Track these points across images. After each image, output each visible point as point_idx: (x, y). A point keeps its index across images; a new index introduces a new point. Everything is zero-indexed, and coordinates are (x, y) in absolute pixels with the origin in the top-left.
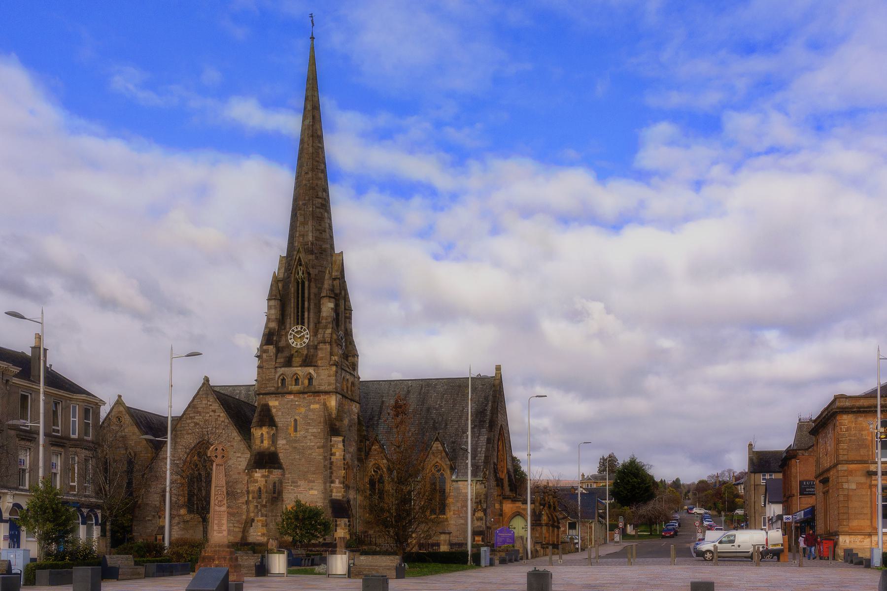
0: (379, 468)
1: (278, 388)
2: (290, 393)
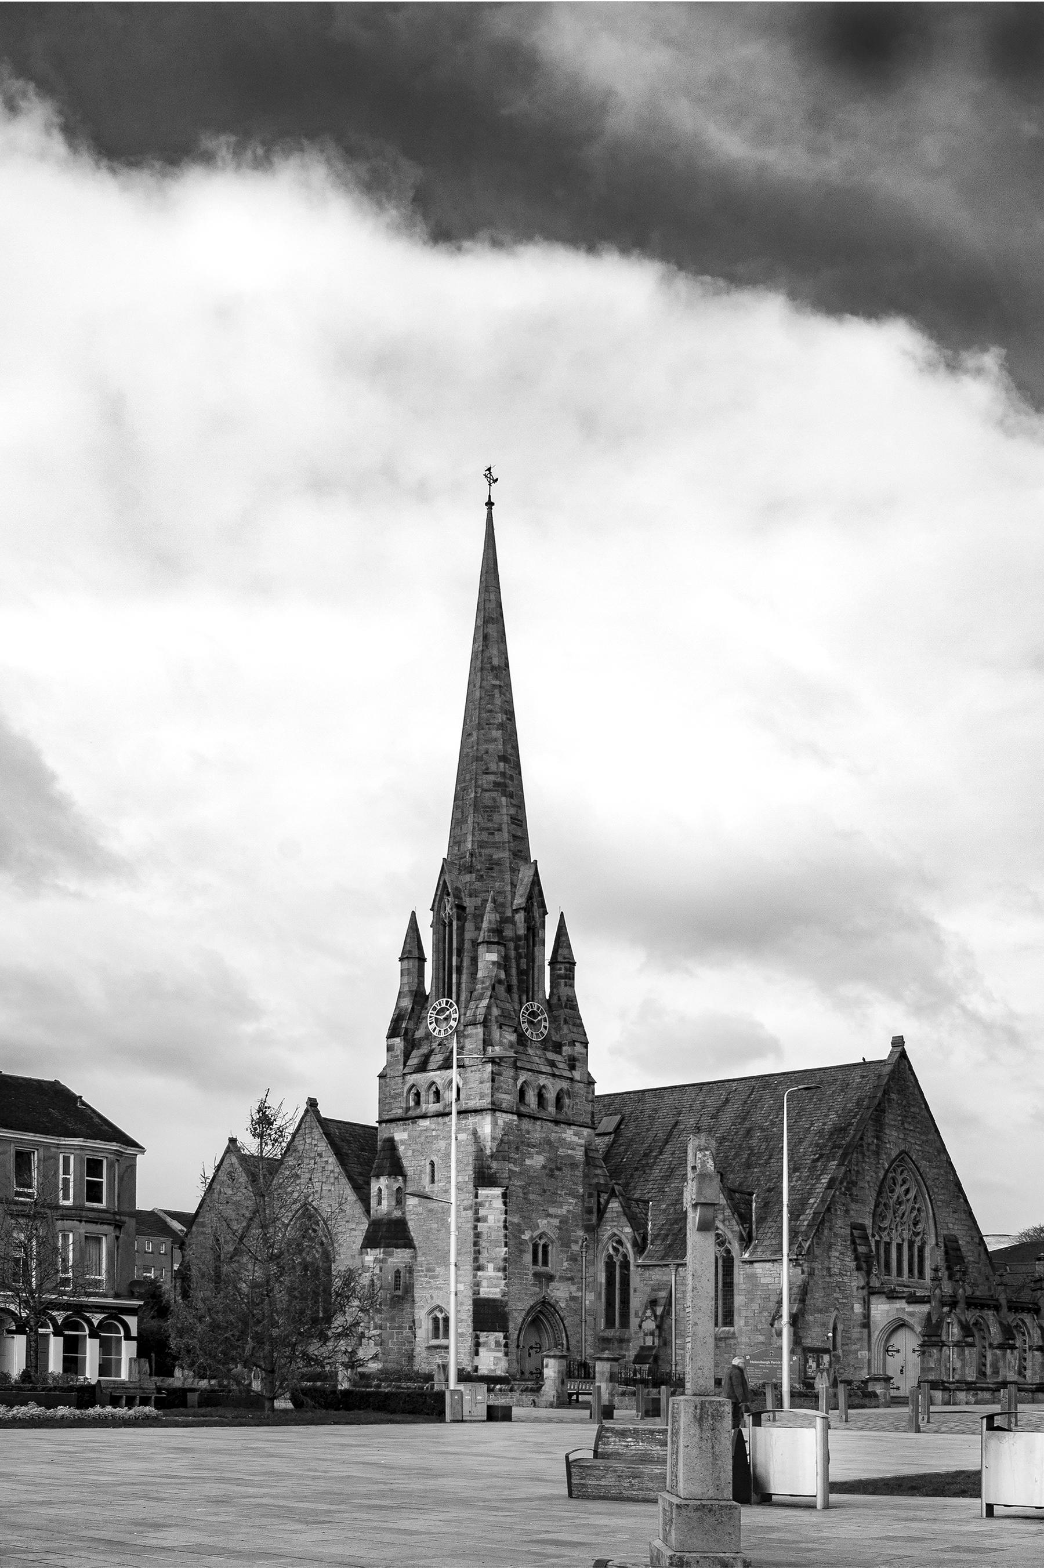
1: (408, 1109)
2: (424, 1117)
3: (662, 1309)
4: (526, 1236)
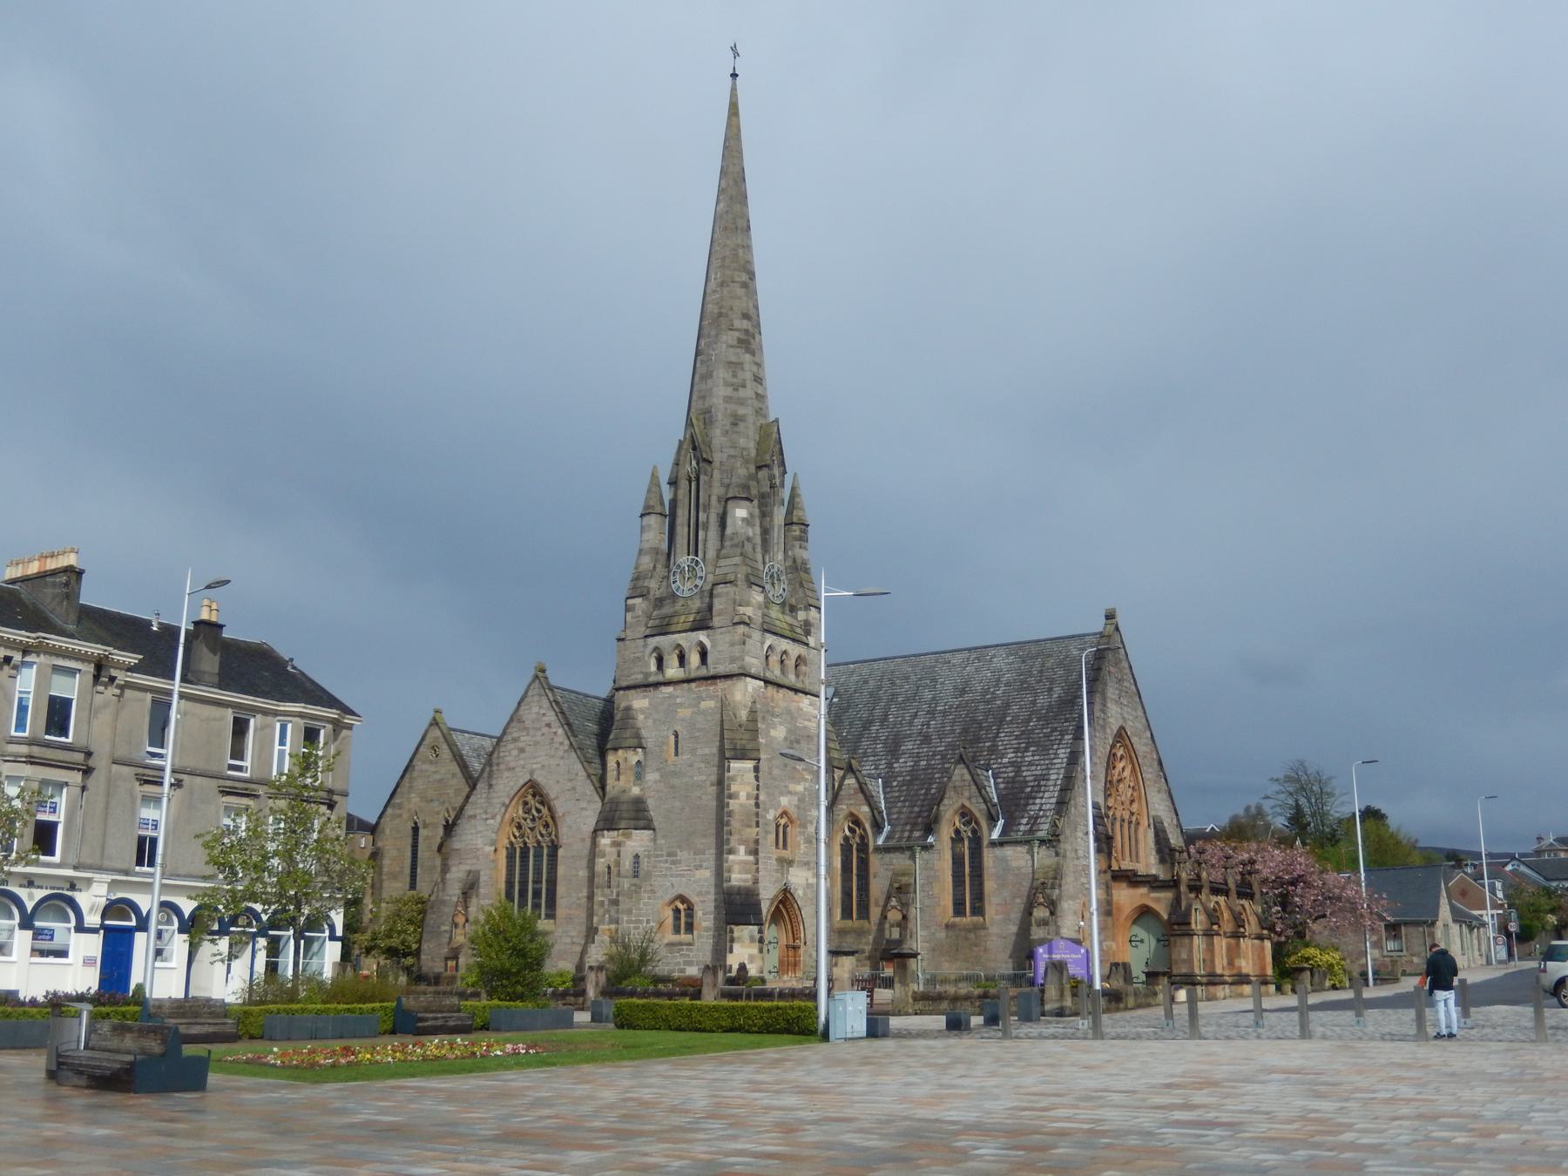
0: (856, 822)
1: (647, 675)
3: (901, 890)
4: (771, 815)
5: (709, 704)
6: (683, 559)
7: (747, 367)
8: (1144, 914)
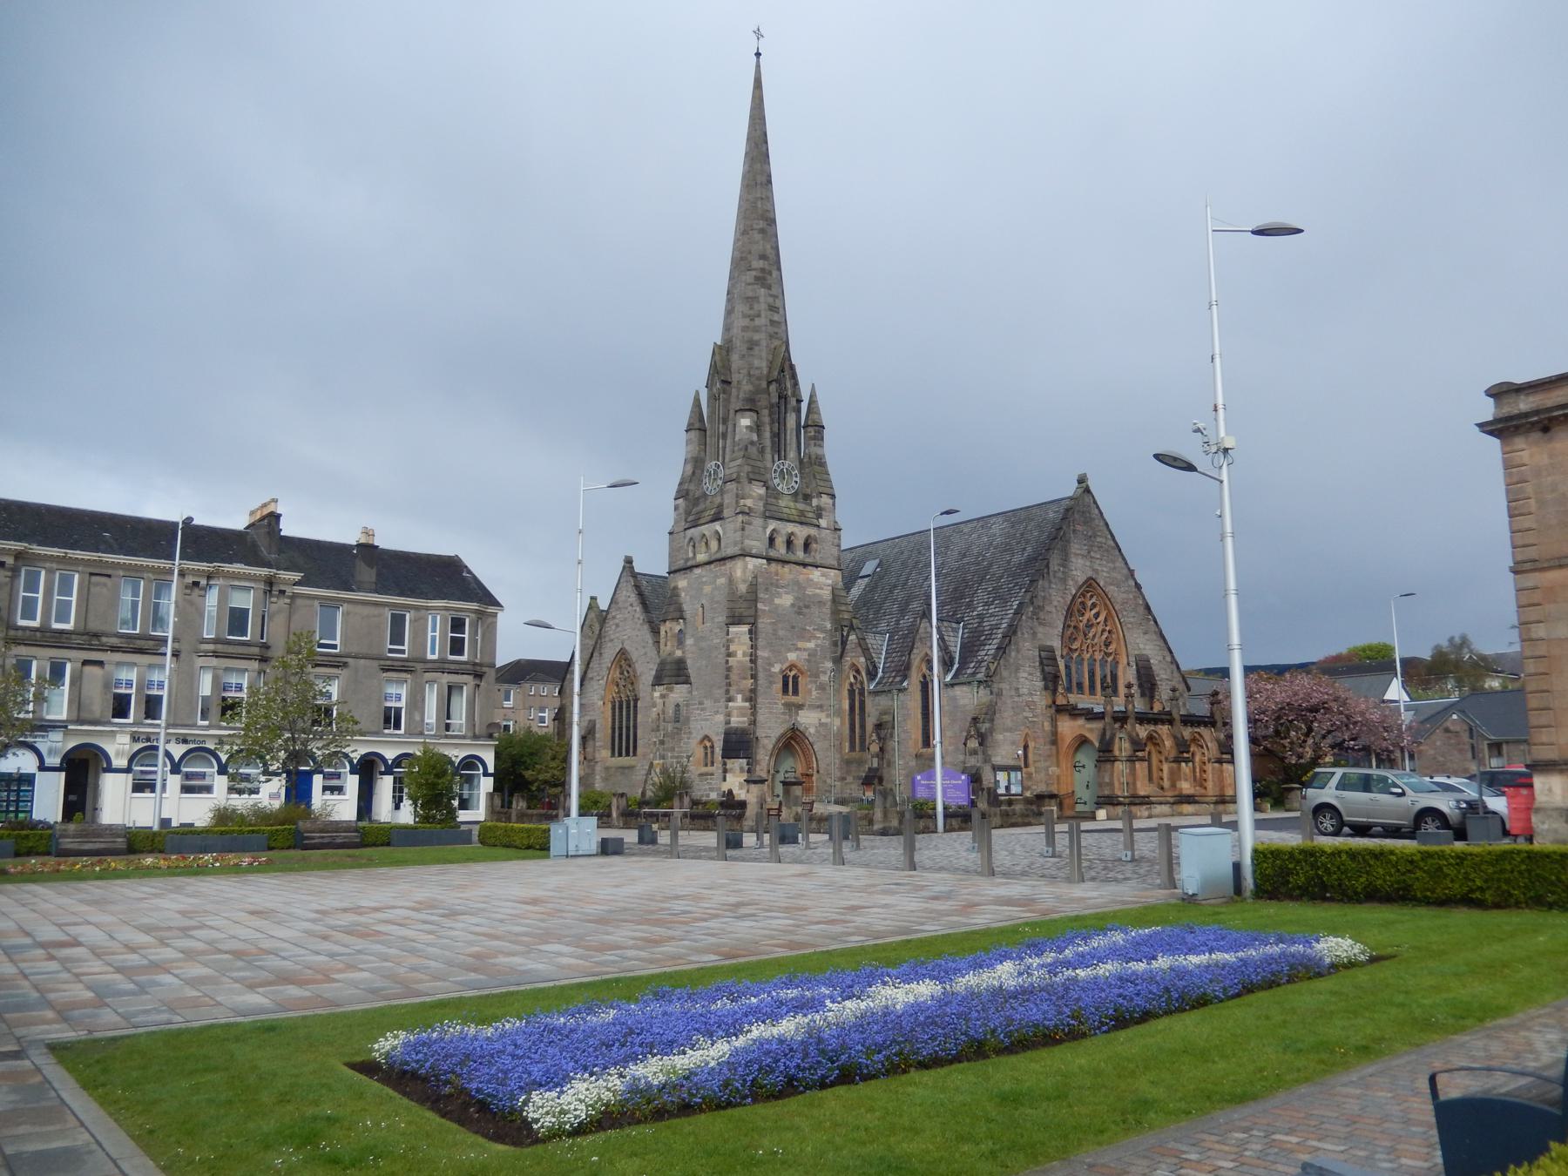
1: (687, 560)
2: (697, 566)
4: (776, 668)
5: (722, 581)
6: (711, 465)
7: (762, 299)
8: (1082, 742)
